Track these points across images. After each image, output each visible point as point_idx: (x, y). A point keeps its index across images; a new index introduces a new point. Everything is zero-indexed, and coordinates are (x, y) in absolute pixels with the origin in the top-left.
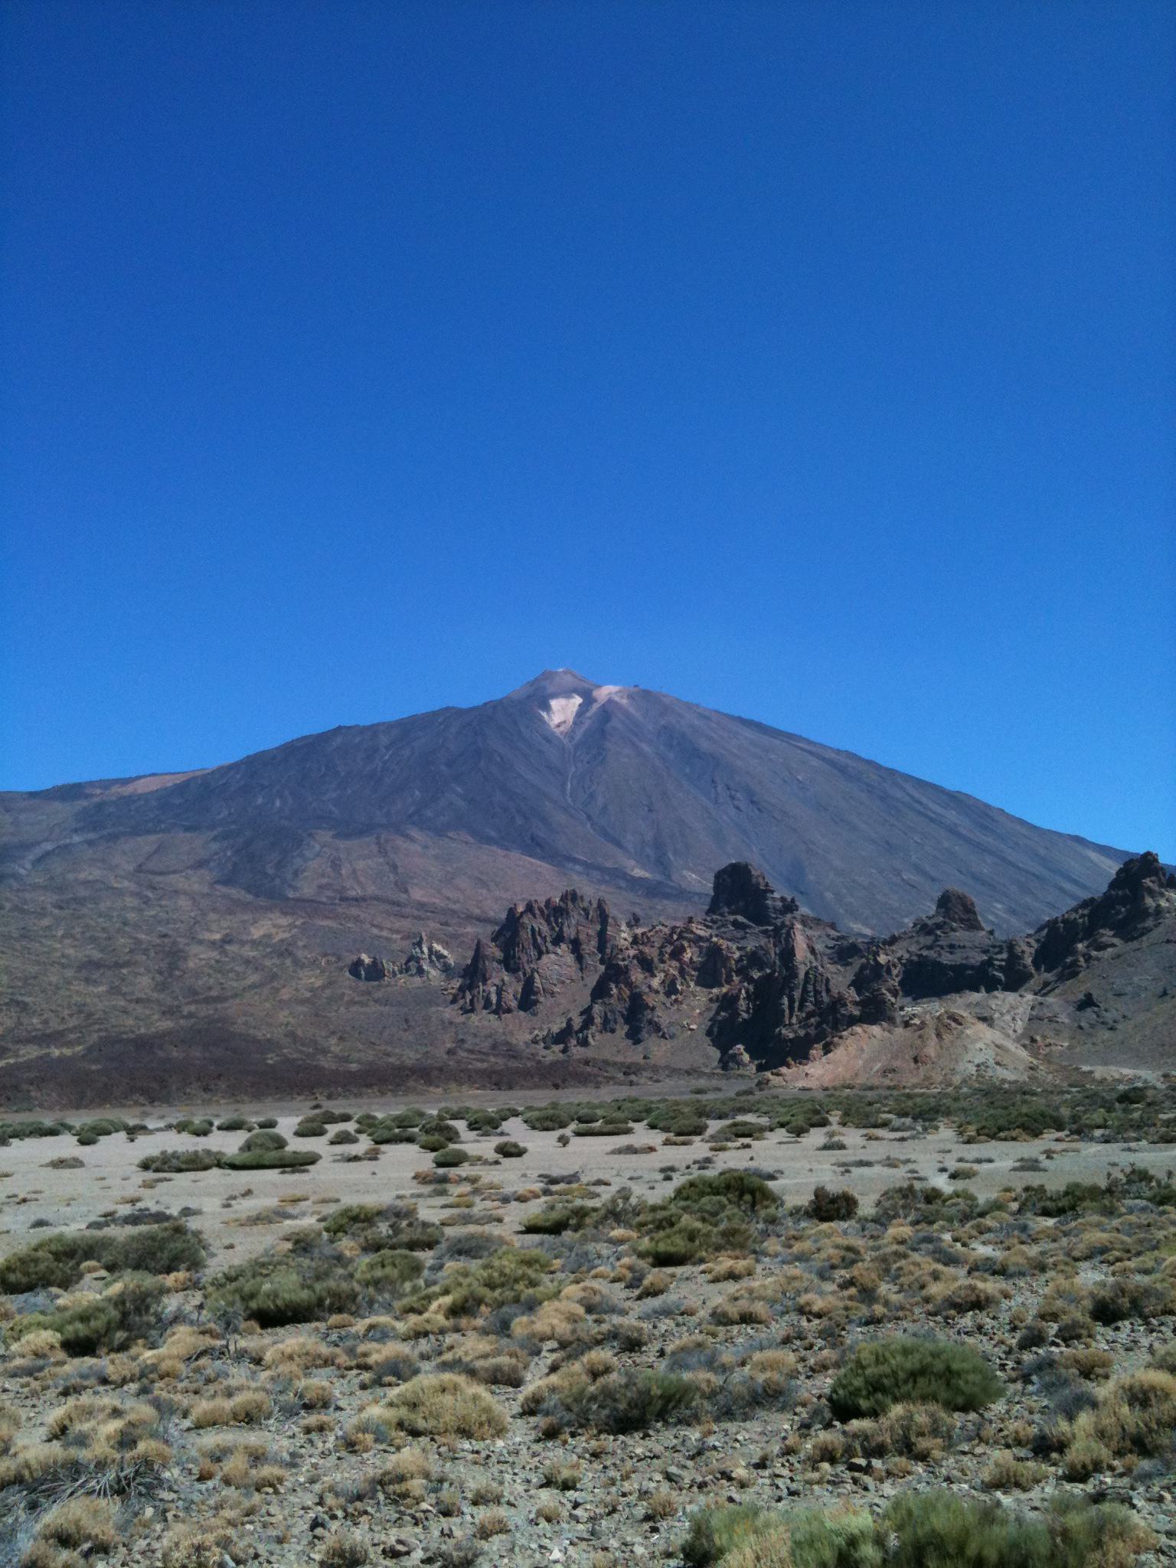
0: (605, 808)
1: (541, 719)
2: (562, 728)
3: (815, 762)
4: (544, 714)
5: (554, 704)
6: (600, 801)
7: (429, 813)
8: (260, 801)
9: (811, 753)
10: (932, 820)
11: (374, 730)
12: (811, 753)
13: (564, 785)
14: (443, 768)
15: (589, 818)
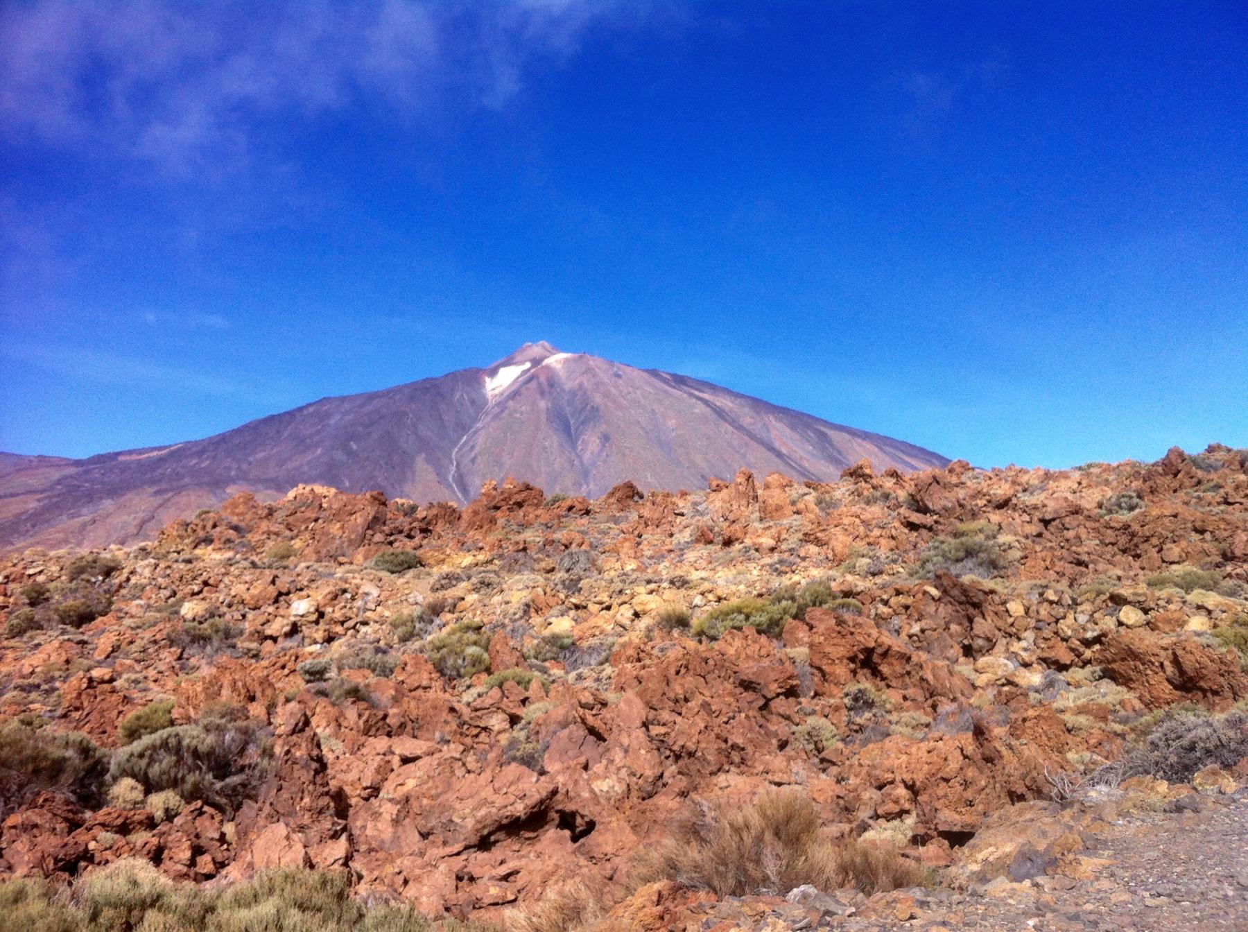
0: (473, 460)
1: (481, 385)
2: (496, 392)
3: (700, 408)
4: (487, 380)
5: (503, 371)
6: (477, 449)
7: (306, 468)
8: (194, 462)
9: (706, 402)
10: (779, 454)
11: (343, 399)
12: (706, 402)
13: (460, 438)
14: (360, 429)
15: (458, 466)
